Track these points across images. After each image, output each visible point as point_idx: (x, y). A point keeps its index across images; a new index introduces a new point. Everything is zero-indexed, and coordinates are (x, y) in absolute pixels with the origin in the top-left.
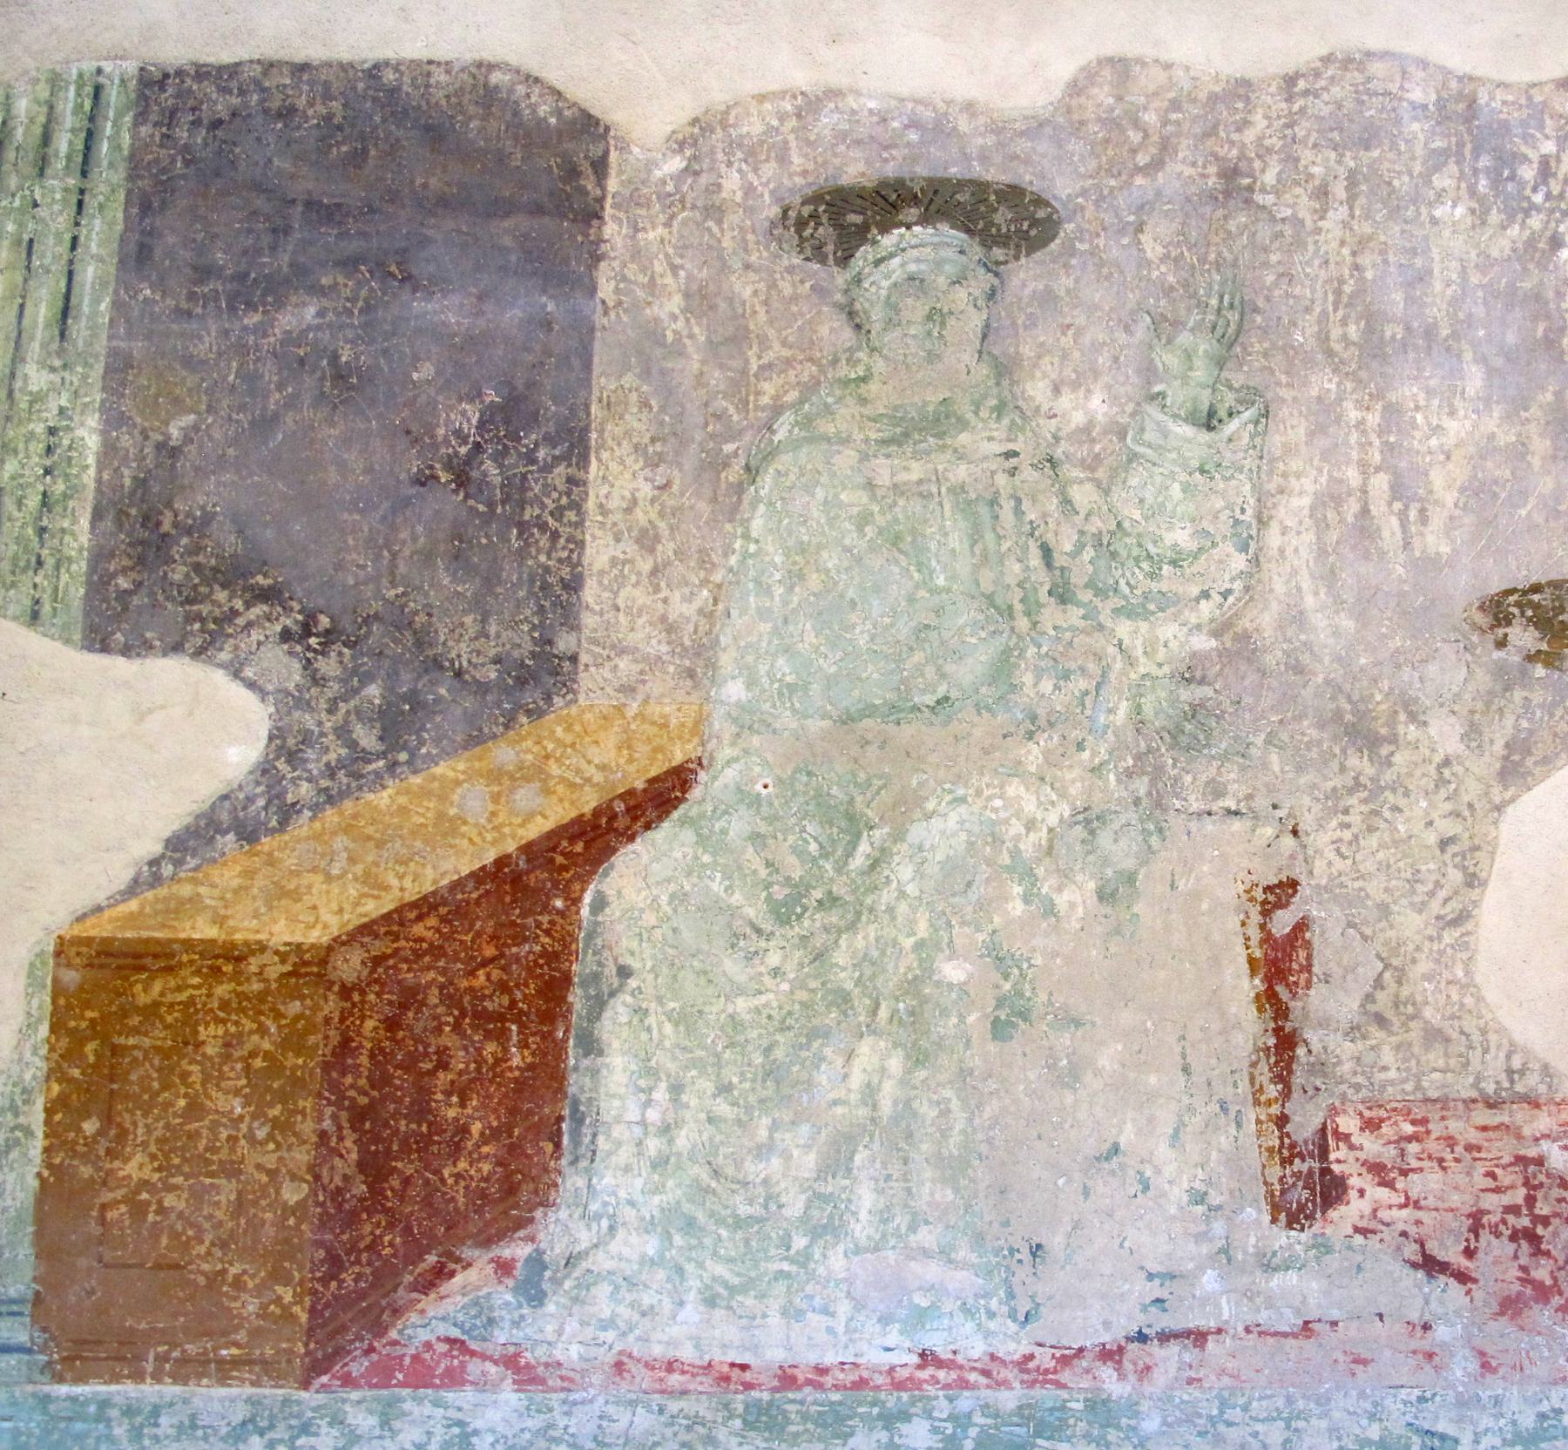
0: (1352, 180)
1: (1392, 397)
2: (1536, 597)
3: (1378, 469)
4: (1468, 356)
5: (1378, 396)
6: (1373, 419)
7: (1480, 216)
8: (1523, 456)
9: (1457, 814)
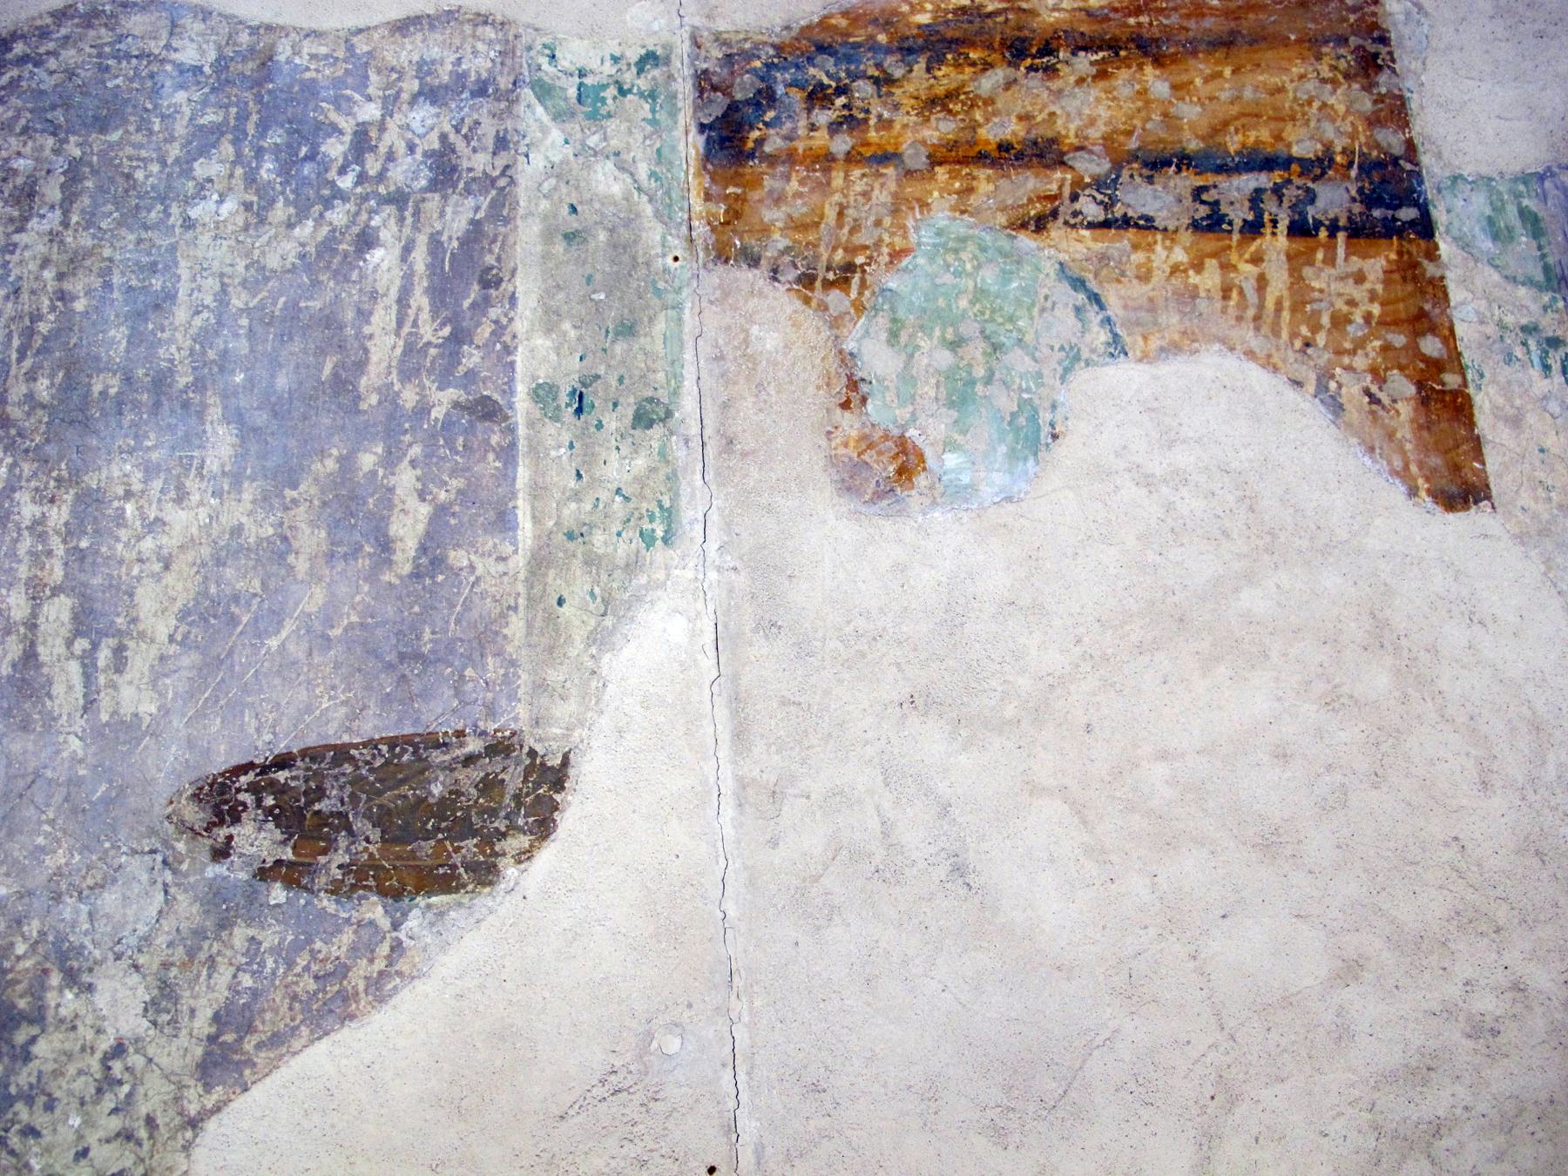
0: (73, 174)
1: (91, 480)
2: (282, 776)
3: (56, 591)
4: (215, 412)
5: (74, 478)
6: (59, 516)
7: (257, 214)
8: (282, 556)
9: (127, 1136)
